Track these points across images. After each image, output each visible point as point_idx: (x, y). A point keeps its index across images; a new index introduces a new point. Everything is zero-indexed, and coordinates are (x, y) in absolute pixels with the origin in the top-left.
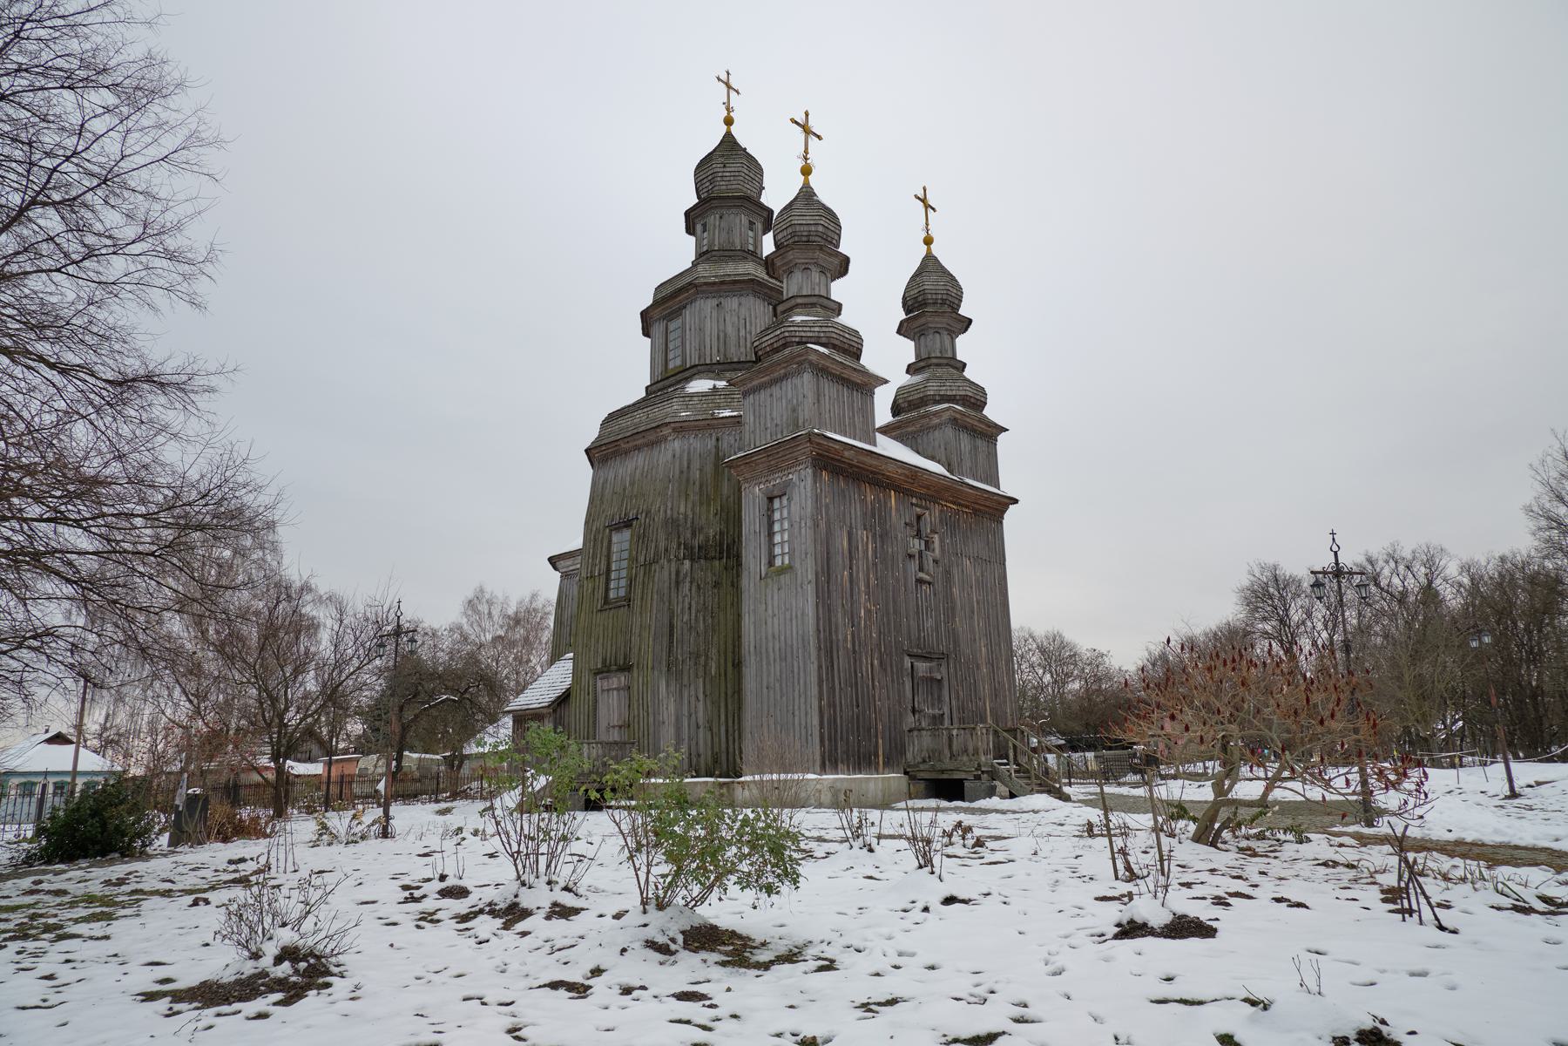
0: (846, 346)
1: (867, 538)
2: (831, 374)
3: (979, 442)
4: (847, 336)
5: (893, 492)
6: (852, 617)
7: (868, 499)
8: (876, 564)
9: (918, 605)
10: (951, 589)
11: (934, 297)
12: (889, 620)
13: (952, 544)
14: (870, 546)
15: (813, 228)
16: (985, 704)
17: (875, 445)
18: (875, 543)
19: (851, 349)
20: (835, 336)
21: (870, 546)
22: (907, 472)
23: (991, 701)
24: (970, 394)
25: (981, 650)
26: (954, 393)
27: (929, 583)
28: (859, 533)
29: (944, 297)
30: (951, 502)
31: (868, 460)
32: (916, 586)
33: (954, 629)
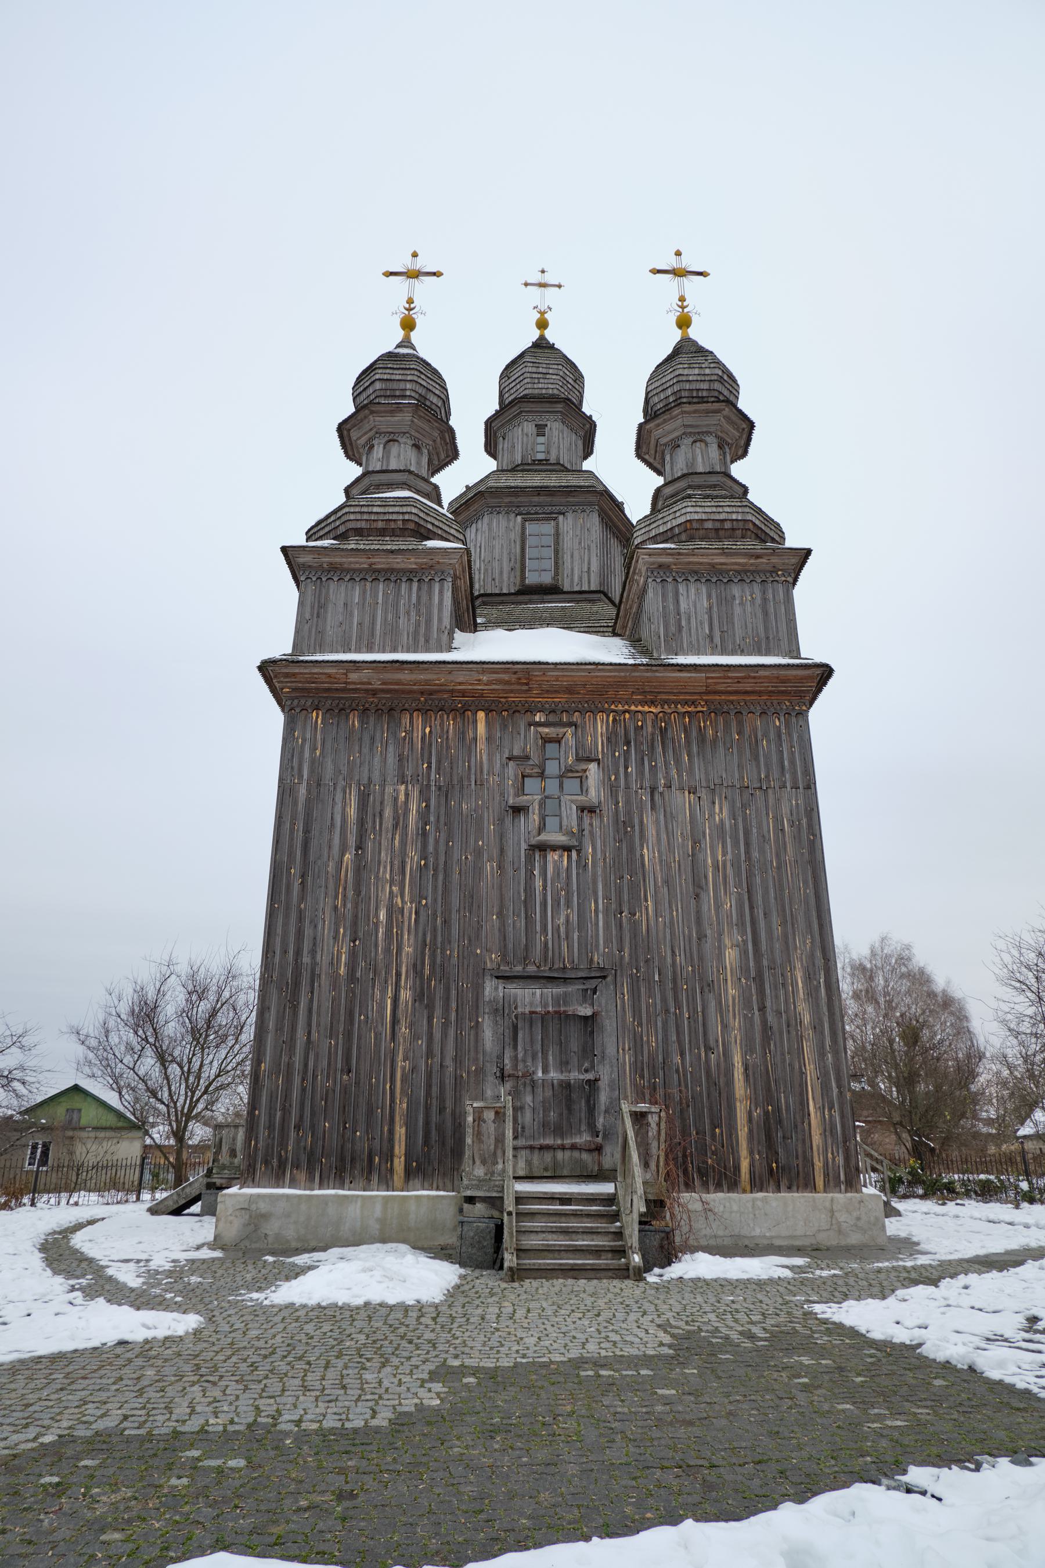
0: (380, 525)
1: (407, 795)
2: (348, 571)
3: (736, 590)
4: (375, 509)
5: (481, 715)
6: (355, 923)
7: (418, 735)
8: (424, 834)
9: (529, 889)
10: (631, 850)
11: (662, 396)
12: (446, 922)
13: (641, 773)
14: (414, 807)
15: (371, 390)
16: (727, 1054)
17: (450, 649)
18: (428, 801)
19: (393, 525)
20: (352, 517)
21: (414, 807)
22: (505, 677)
23: (748, 1048)
24: (696, 517)
25: (720, 957)
26: (669, 526)
27: (568, 849)
28: (389, 789)
29: (676, 388)
30: (643, 703)
31: (405, 676)
32: (530, 860)
33: (635, 926)
